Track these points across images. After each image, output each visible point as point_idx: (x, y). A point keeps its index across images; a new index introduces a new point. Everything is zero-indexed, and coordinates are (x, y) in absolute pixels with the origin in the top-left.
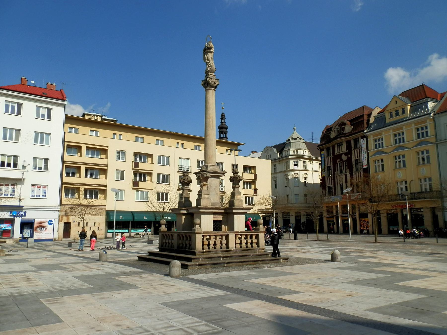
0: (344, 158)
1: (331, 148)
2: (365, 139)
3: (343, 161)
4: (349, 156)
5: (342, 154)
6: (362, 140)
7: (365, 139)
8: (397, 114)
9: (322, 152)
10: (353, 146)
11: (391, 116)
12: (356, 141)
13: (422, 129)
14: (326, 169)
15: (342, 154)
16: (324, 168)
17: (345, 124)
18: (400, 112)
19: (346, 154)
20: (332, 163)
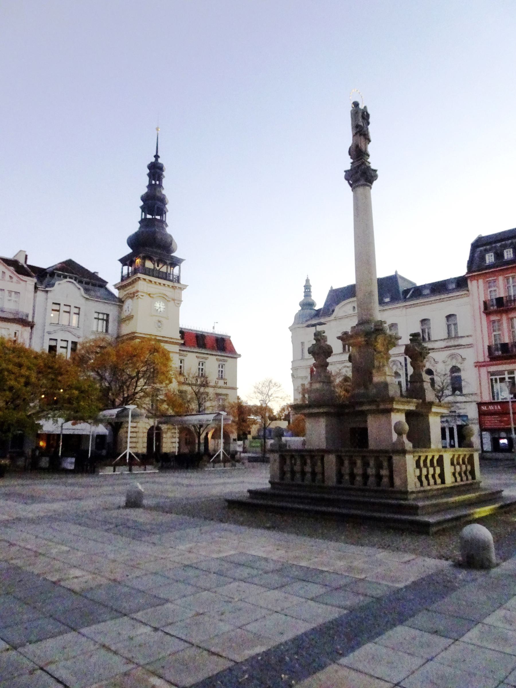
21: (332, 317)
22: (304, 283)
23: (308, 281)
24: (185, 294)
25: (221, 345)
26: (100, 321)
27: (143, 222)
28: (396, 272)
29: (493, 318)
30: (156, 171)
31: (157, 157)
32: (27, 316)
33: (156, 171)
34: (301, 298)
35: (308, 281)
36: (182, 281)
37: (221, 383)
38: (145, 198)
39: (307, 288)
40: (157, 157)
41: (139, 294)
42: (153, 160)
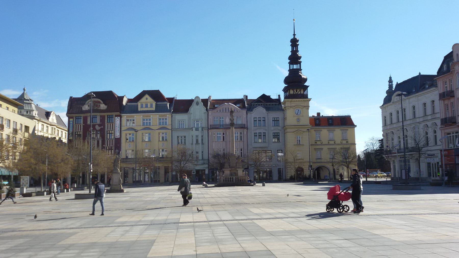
0: (97, 128)
1: (82, 118)
2: (119, 118)
3: (97, 131)
4: (102, 127)
5: (96, 125)
6: (116, 118)
7: (119, 118)
8: (147, 106)
9: (71, 120)
10: (106, 121)
11: (142, 107)
12: (110, 117)
13: (163, 119)
14: (74, 134)
15: (96, 125)
16: (73, 132)
17: (100, 102)
18: (149, 106)
19: (99, 125)
20: (82, 130)
21: (391, 103)
22: (388, 79)
23: (390, 78)
24: (311, 103)
25: (345, 122)
26: (276, 122)
27: (290, 70)
28: (420, 73)
29: (446, 102)
30: (294, 42)
31: (294, 35)
32: (245, 125)
33: (294, 42)
34: (387, 88)
35: (390, 78)
36: (309, 97)
37: (344, 142)
38: (290, 58)
39: (390, 81)
40: (294, 35)
41: (287, 108)
42: (292, 37)
